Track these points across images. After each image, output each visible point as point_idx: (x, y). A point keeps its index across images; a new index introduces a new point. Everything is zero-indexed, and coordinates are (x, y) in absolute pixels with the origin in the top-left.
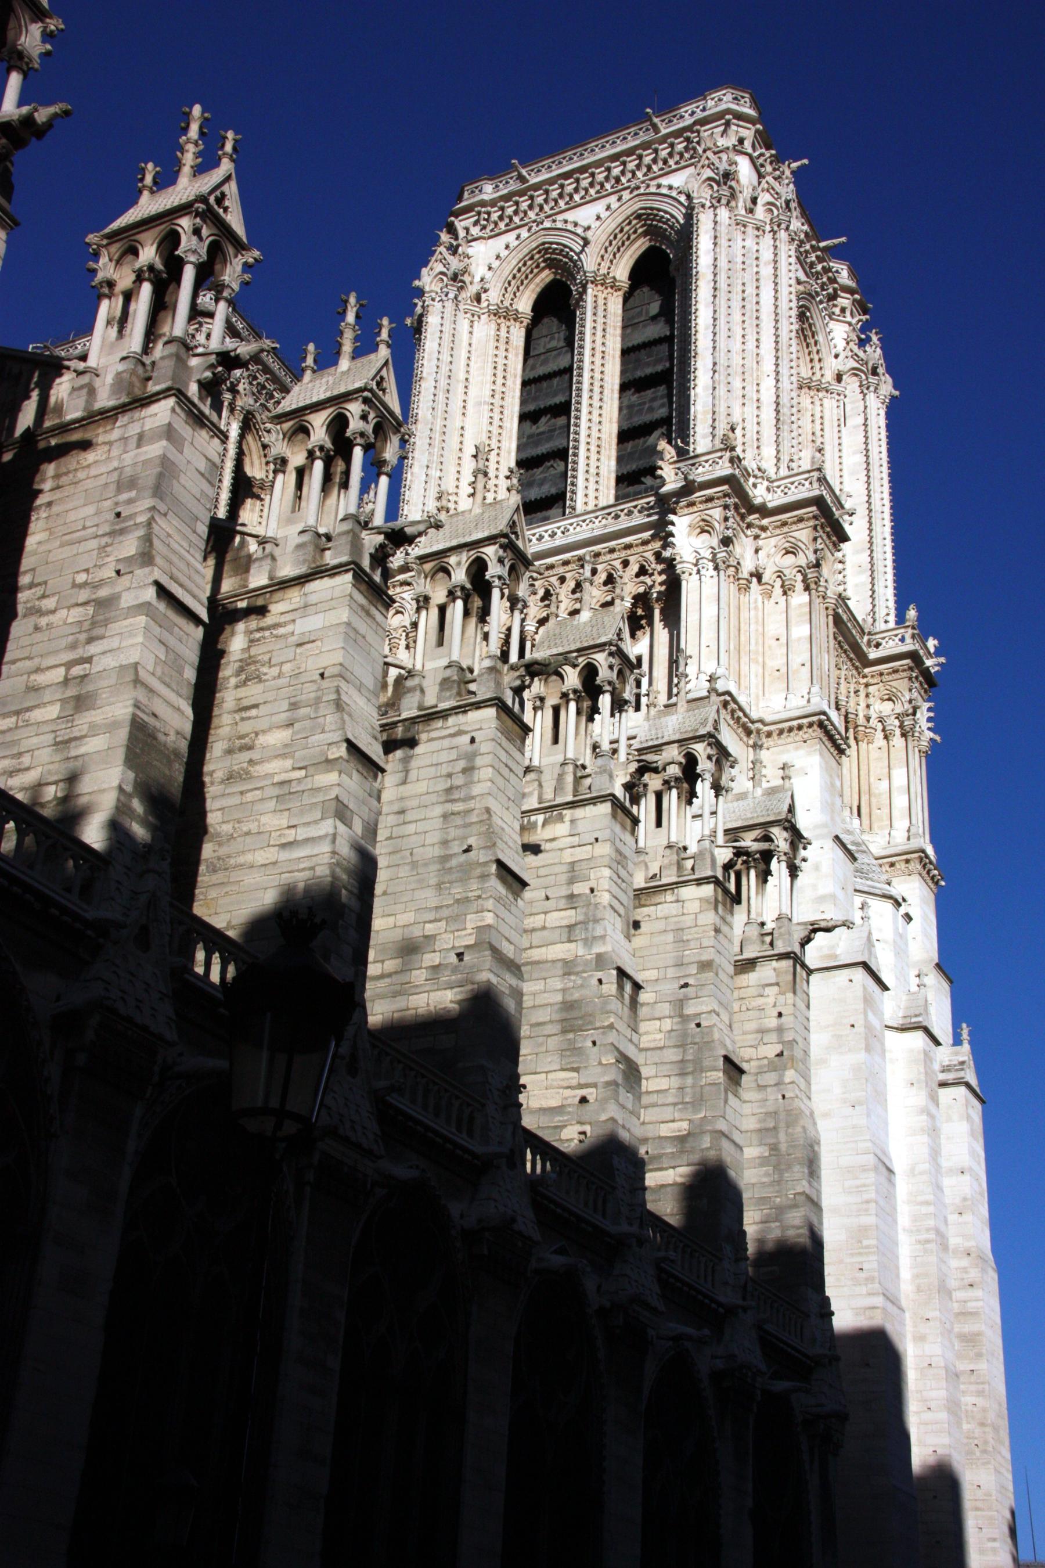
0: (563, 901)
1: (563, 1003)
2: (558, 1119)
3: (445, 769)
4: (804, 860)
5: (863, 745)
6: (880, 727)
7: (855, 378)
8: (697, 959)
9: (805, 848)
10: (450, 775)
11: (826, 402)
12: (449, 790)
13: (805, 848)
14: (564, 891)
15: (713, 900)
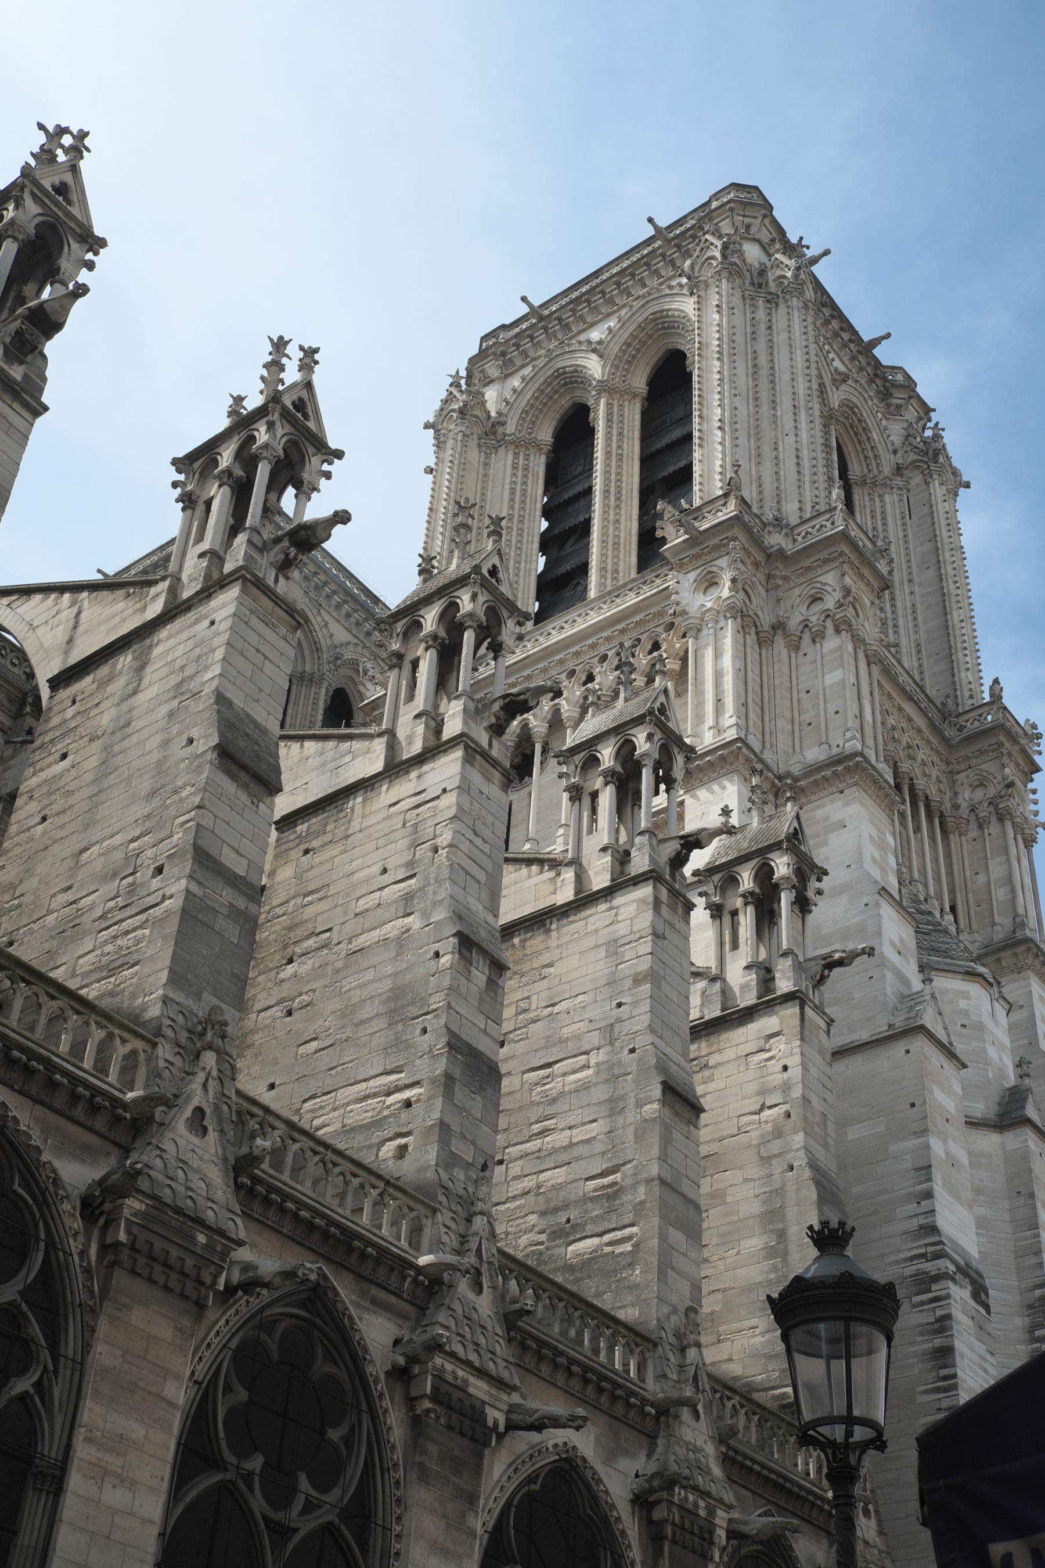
0: (403, 870)
1: (391, 990)
2: (377, 1136)
3: (178, 663)
4: (819, 892)
5: (954, 839)
6: (973, 818)
7: (917, 472)
8: (632, 972)
9: (819, 880)
10: (182, 668)
11: (887, 498)
12: (179, 685)
13: (819, 880)
14: (405, 857)
15: (651, 899)
